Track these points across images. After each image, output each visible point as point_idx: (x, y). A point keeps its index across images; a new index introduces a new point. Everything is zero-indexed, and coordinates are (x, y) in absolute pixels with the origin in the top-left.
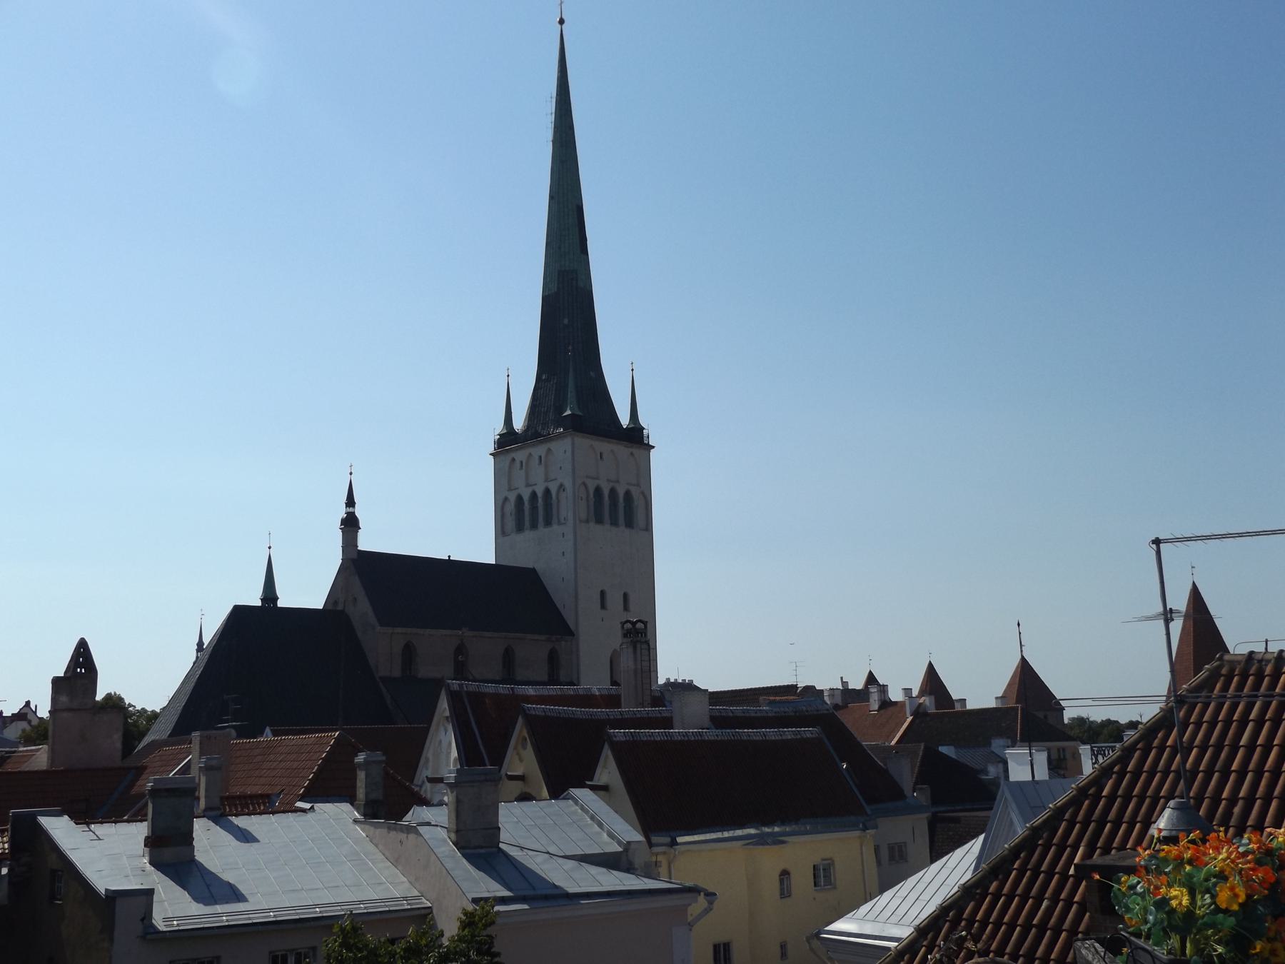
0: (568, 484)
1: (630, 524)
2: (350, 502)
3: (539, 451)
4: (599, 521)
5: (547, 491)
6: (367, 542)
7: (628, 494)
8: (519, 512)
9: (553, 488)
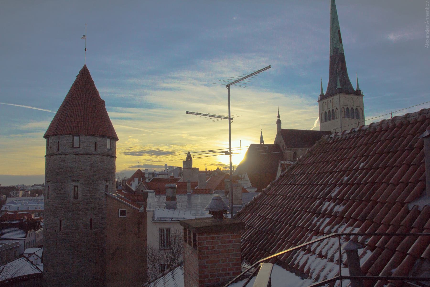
0: (338, 108)
1: (358, 118)
2: (279, 116)
3: (330, 99)
4: (348, 117)
5: (333, 110)
6: (283, 127)
7: (357, 109)
8: (326, 117)
9: (335, 109)
